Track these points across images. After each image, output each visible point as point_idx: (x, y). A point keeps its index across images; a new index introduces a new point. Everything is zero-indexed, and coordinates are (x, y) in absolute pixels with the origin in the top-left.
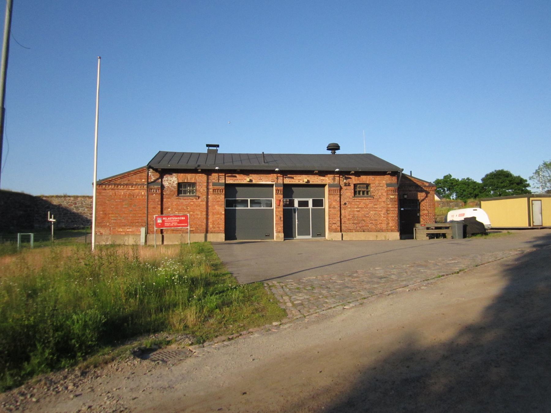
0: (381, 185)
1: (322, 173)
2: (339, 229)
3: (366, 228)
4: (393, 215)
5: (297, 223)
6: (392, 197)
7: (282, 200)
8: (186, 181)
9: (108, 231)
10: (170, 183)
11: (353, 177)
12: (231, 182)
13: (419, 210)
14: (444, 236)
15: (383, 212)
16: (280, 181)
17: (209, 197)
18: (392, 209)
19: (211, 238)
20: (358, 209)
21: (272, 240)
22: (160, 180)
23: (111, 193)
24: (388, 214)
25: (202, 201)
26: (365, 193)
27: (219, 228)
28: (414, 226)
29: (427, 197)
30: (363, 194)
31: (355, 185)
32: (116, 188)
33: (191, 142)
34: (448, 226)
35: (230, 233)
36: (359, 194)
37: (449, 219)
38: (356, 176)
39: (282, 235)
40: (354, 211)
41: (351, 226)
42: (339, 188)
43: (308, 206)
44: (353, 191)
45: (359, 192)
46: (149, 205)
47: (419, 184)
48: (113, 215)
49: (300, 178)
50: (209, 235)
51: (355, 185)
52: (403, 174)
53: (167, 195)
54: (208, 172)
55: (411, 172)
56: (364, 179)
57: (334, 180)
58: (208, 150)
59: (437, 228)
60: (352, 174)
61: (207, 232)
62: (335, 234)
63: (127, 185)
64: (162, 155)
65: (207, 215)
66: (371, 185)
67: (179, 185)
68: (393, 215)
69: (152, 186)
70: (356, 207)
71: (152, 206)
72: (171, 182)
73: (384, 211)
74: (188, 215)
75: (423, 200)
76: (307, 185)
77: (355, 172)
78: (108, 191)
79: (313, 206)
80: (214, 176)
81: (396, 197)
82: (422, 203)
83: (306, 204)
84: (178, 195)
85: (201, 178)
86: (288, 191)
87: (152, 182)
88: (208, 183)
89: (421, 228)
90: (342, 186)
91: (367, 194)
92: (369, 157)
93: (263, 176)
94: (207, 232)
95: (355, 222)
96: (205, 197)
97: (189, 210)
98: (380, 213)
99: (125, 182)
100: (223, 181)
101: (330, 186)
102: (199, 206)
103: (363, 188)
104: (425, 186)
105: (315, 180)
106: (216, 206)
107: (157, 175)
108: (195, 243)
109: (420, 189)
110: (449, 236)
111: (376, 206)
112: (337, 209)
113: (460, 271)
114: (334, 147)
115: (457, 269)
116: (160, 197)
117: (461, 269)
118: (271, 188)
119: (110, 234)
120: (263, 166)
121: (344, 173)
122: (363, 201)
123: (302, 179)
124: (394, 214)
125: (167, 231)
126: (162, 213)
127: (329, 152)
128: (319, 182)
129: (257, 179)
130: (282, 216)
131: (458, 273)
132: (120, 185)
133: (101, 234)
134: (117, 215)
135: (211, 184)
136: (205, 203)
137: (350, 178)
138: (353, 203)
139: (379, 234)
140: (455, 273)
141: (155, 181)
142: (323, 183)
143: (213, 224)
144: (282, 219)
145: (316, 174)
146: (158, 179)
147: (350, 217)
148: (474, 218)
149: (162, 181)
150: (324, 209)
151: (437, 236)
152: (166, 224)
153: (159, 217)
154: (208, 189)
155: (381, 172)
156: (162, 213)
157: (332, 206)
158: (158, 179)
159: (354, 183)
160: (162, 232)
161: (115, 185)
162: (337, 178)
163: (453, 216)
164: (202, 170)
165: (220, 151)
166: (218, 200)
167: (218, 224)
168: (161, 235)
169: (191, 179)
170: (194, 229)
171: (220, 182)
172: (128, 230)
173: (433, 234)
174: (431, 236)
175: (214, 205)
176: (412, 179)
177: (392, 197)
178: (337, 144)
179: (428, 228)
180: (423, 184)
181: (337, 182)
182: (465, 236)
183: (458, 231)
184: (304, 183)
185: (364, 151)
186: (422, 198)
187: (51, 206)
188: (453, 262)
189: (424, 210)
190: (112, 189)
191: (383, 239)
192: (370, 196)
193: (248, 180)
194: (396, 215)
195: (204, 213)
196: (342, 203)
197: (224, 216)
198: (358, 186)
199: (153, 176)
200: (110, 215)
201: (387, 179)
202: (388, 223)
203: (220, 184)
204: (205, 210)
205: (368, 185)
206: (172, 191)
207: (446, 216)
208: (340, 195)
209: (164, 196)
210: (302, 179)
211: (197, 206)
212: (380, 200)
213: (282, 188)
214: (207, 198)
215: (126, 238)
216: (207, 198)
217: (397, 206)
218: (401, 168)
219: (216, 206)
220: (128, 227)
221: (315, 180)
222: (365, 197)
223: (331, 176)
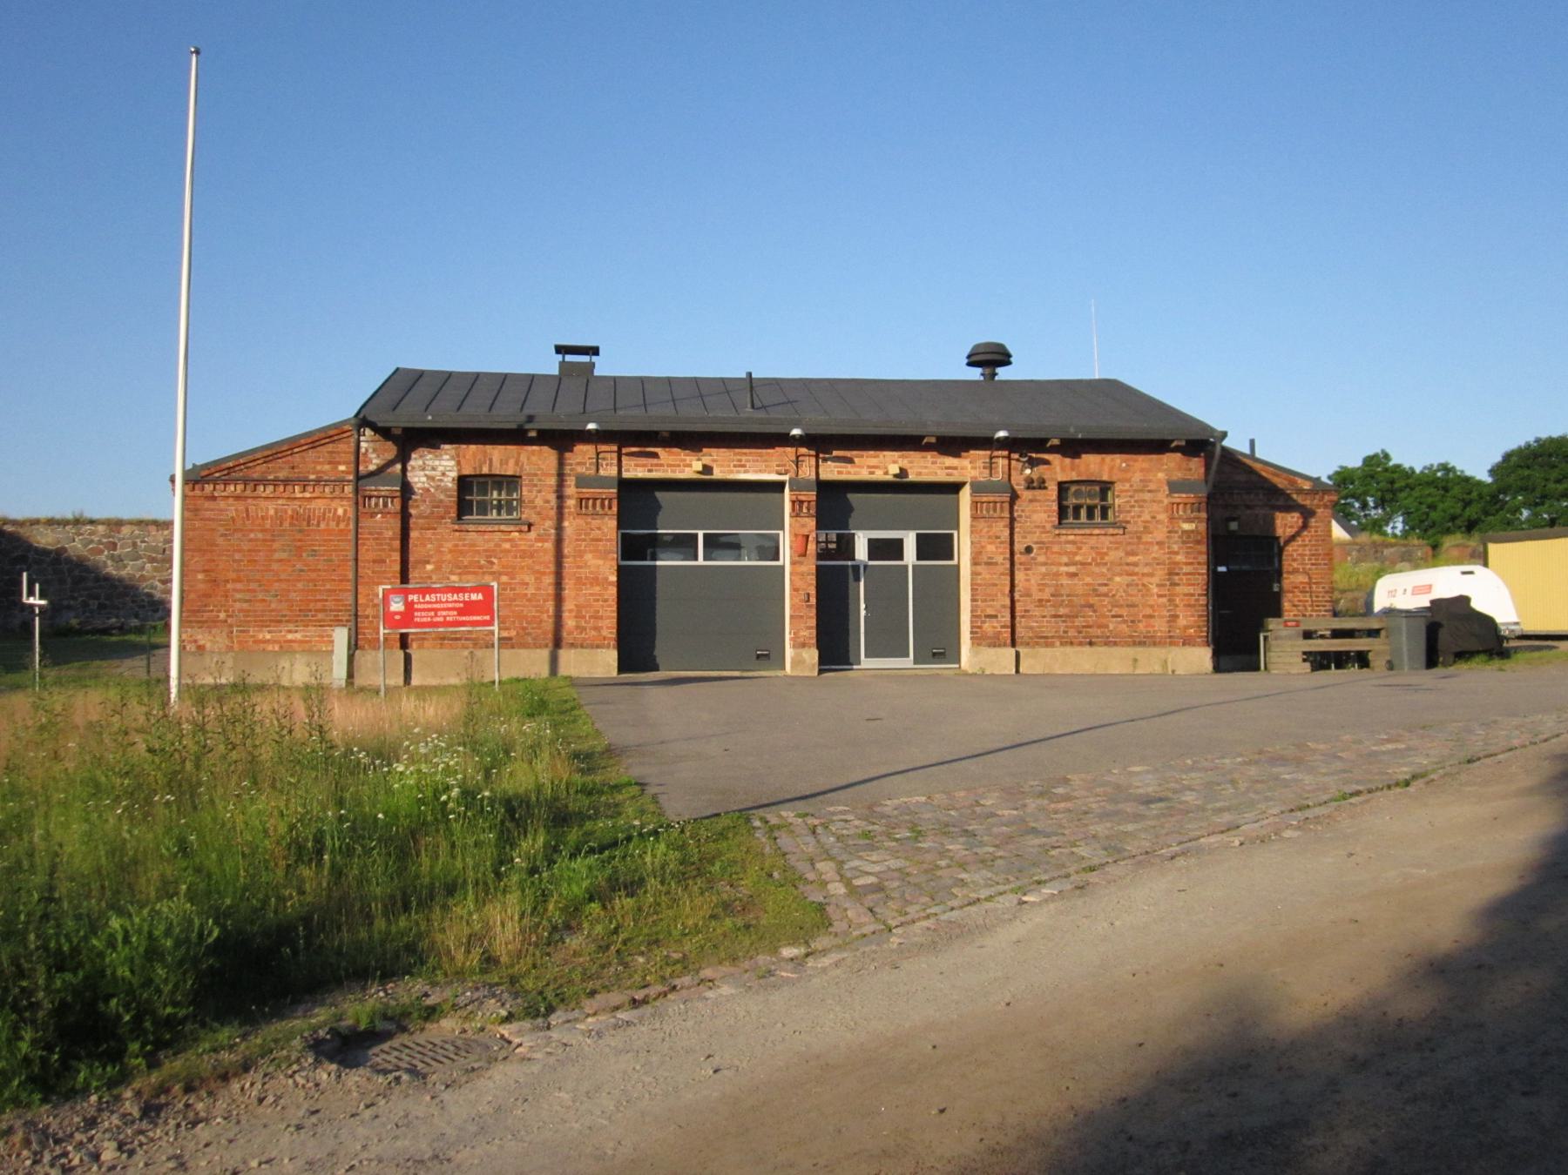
0: (1152, 486)
1: (952, 445)
2: (1006, 634)
3: (1099, 632)
4: (1191, 590)
5: (863, 613)
6: (1186, 526)
7: (813, 535)
8: (485, 470)
9: (222, 640)
11: (1055, 458)
12: (641, 474)
13: (1279, 573)
14: (1362, 660)
15: (1155, 580)
16: (807, 472)
17: (566, 524)
18: (1186, 569)
19: (573, 663)
20: (1072, 569)
21: (780, 673)
22: (399, 466)
23: (232, 509)
24: (1174, 584)
25: (540, 539)
26: (1097, 512)
27: (597, 629)
28: (1260, 626)
29: (1305, 526)
30: (1090, 515)
31: (1063, 488)
32: (248, 493)
33: (502, 338)
34: (1376, 626)
35: (636, 651)
36: (1077, 516)
37: (1379, 604)
38: (1065, 455)
39: (812, 655)
40: (1057, 574)
42: (1006, 497)
43: (901, 557)
44: (1055, 507)
45: (1077, 509)
46: (362, 550)
47: (1280, 482)
48: (239, 586)
49: (873, 461)
50: (565, 655)
51: (1063, 488)
52: (1224, 449)
53: (420, 516)
54: (562, 440)
55: (1252, 443)
56: (1094, 465)
57: (991, 467)
58: (563, 364)
59: (1337, 634)
60: (1053, 450)
61: (557, 643)
62: (992, 651)
63: (286, 482)
64: (404, 383)
65: (559, 584)
66: (1118, 487)
67: (464, 483)
68: (1191, 590)
69: (370, 488)
70: (1064, 561)
71: (371, 556)
72: (437, 474)
73: (1161, 573)
74: (495, 585)
75: (1293, 538)
76: (901, 485)
77: (1062, 440)
78: (222, 504)
79: (919, 558)
80: (583, 455)
81: (1203, 527)
82: (1289, 548)
83: (891, 549)
84: (459, 517)
85: (536, 462)
86: (833, 503)
87: (372, 474)
88: (561, 476)
89: (1285, 632)
90: (1020, 487)
91: (1104, 515)
92: (1111, 390)
93: (748, 455)
94: (557, 643)
95: (1062, 611)
96: (549, 524)
97: (495, 568)
98: (1146, 580)
99: (282, 475)
100: (613, 471)
101: (978, 488)
102: (532, 556)
103: (1090, 496)
104: (1300, 491)
105: (926, 467)
106: (588, 557)
107: (390, 450)
108: (518, 680)
109: (1281, 502)
110: (1378, 662)
112: (1001, 569)
113: (1415, 777)
114: (991, 358)
115: (1404, 772)
116: (396, 523)
117: (1418, 771)
118: (777, 495)
119: (230, 649)
120: (747, 418)
121: (1026, 446)
122: (1088, 542)
123: (883, 466)
125: (422, 638)
126: (404, 578)
127: (976, 374)
128: (941, 477)
129: (727, 465)
130: (813, 592)
131: (1407, 784)
132: (264, 482)
133: (201, 648)
134: (253, 586)
135: (571, 482)
136: (549, 545)
137: (1047, 462)
138: (1056, 548)
140: (1397, 784)
141: (381, 470)
142: (955, 477)
143: (578, 616)
144: (813, 601)
145: (928, 448)
146: (391, 463)
147: (1046, 595)
148: (1463, 601)
149: (404, 470)
150: (958, 567)
151: (1340, 660)
152: (419, 617)
153: (395, 591)
154: (561, 498)
155: (1152, 441)
156: (404, 578)
158: (391, 463)
159: (1061, 478)
160: (404, 642)
161: (246, 482)
162: (1001, 463)
163: (1392, 593)
164: (541, 433)
165: (604, 367)
167: (596, 617)
168: (401, 654)
169: (504, 462)
170: (513, 633)
171: (602, 472)
172: (290, 636)
173: (1324, 654)
174: (1320, 661)
175: (580, 554)
176: (1257, 466)
177: (1186, 526)
178: (1002, 346)
179: (1308, 635)
180: (1293, 483)
181: (999, 476)
182: (1431, 663)
183: (1410, 644)
184: (889, 478)
185: (1095, 370)
186: (1290, 532)
187: (31, 555)
188: (1390, 746)
189: (1295, 571)
190: (238, 498)
191: (1158, 669)
192: (1114, 525)
193: (698, 466)
195: (549, 580)
196: (1019, 547)
197: (613, 591)
198: (1073, 488)
199: (374, 452)
200: (229, 586)
201: (1170, 466)
203: (602, 482)
204: (552, 568)
205: (1105, 487)
206: (438, 504)
207: (1371, 594)
208: (1012, 520)
209: (412, 521)
210: (883, 466)
211: (524, 554)
214: (559, 529)
215: (284, 663)
217: (1203, 558)
218: (1220, 428)
219: (588, 557)
220: (291, 626)
221: (926, 467)
222: (1097, 526)
223: (981, 455)
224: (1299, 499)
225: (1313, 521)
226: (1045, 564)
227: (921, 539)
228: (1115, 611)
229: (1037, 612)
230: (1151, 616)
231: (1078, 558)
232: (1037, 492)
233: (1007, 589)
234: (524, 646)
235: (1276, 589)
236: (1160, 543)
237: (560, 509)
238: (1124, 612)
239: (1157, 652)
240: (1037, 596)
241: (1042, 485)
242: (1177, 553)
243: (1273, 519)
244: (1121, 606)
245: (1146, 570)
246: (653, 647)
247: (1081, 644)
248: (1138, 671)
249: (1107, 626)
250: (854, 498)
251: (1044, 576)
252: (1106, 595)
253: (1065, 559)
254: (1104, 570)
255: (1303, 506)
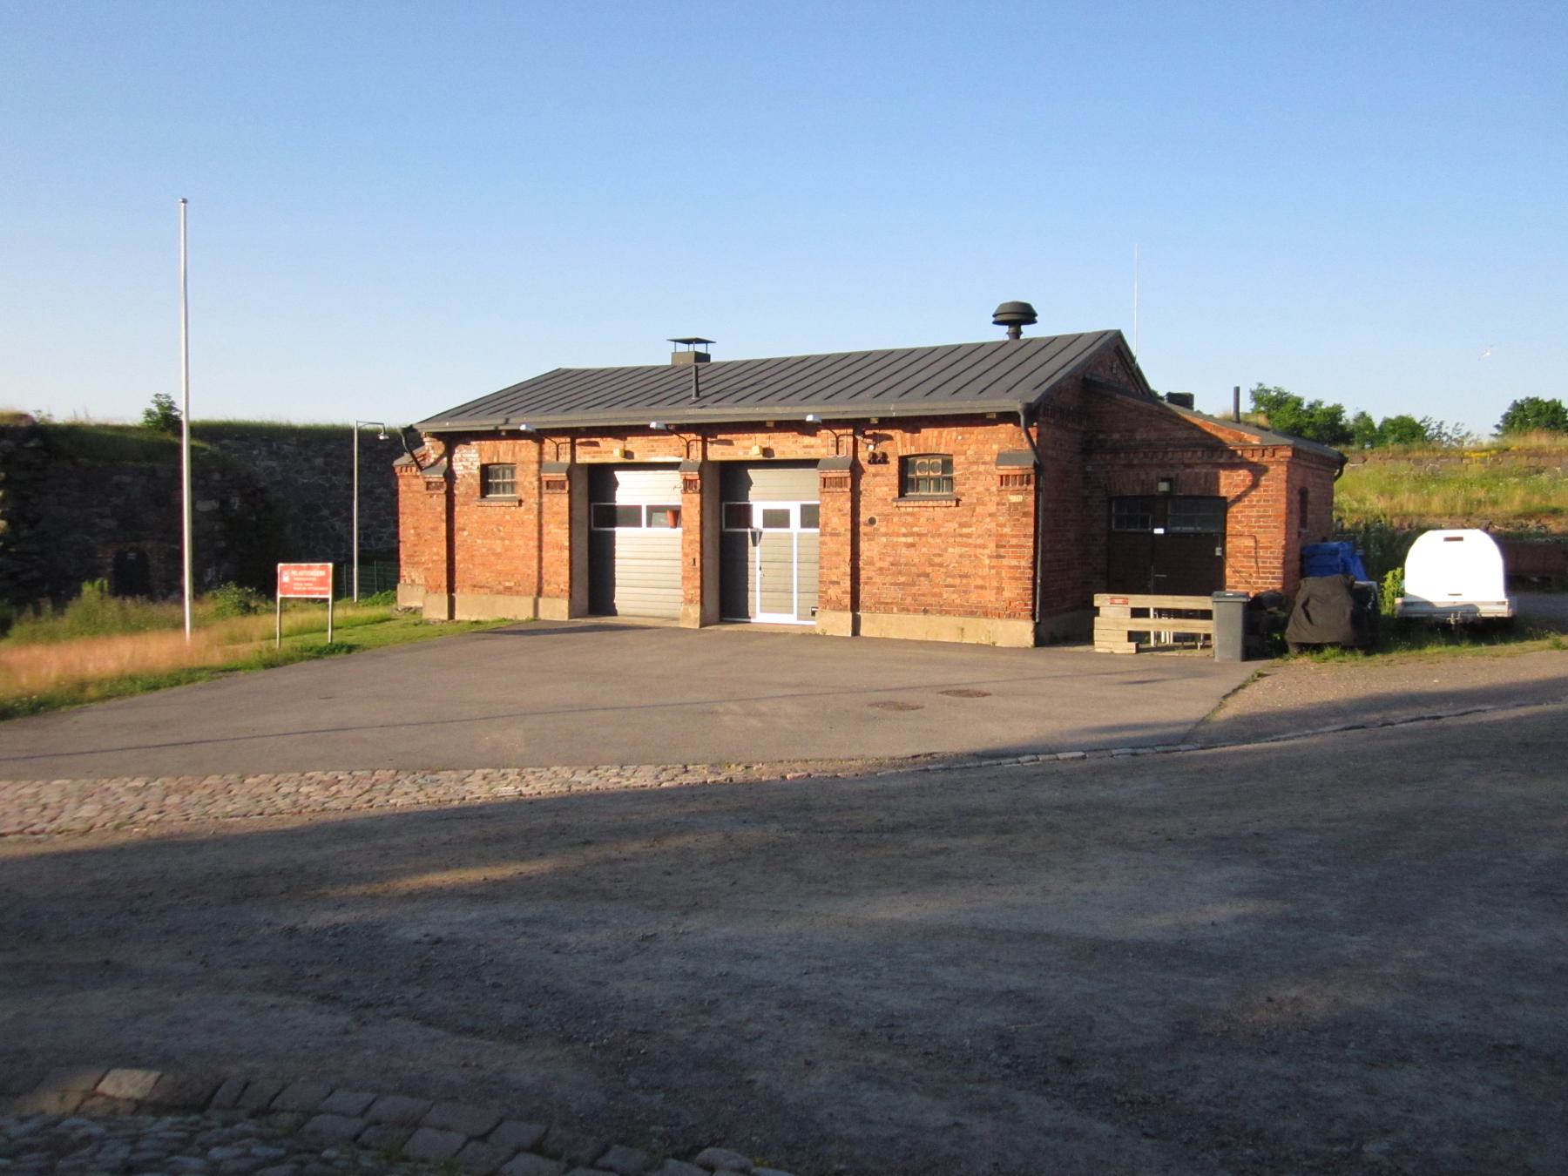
0: (987, 458)
2: (847, 600)
4: (1014, 562)
5: (758, 573)
6: (1015, 499)
10: (465, 467)
11: (897, 434)
13: (1224, 536)
15: (987, 551)
20: (910, 540)
24: (999, 557)
29: (1255, 485)
31: (904, 461)
38: (905, 431)
40: (894, 546)
41: (890, 594)
42: (847, 473)
44: (896, 481)
49: (747, 443)
54: (539, 436)
56: (932, 439)
58: (675, 355)
61: (540, 593)
65: (540, 548)
66: (955, 460)
67: (485, 470)
70: (899, 529)
75: (1239, 499)
79: (803, 525)
80: (549, 445)
82: (1233, 510)
84: (483, 496)
85: (528, 449)
87: (432, 465)
90: (864, 463)
95: (902, 579)
96: (532, 502)
98: (979, 551)
100: (568, 458)
103: (932, 468)
111: (965, 530)
114: (1019, 315)
116: (443, 500)
122: (926, 511)
124: (1021, 558)
127: (1002, 333)
130: (698, 557)
137: (890, 438)
138: (896, 519)
139: (969, 623)
141: (437, 462)
142: (812, 455)
146: (441, 457)
147: (885, 565)
149: (450, 462)
157: (829, 529)
164: (508, 432)
166: (556, 508)
167: (558, 574)
169: (506, 454)
171: (561, 460)
176: (1197, 421)
177: (1015, 499)
194: (1026, 562)
196: (863, 518)
202: (1000, 590)
205: (947, 464)
206: (470, 486)
212: (979, 509)
213: (695, 475)
214: (540, 505)
216: (540, 505)
224: (1248, 455)
225: (1263, 480)
226: (886, 535)
227: (804, 509)
228: (949, 581)
229: (878, 579)
230: (982, 587)
231: (916, 529)
232: (880, 467)
233: (848, 558)
234: (518, 593)
235: (1218, 553)
236: (990, 515)
237: (540, 487)
238: (957, 581)
239: (984, 622)
240: (879, 564)
241: (884, 460)
242: (1004, 526)
243: (1217, 478)
244: (953, 577)
245: (979, 541)
246: (613, 596)
247: (915, 611)
248: (966, 641)
249: (941, 595)
250: (751, 472)
251: (885, 546)
252: (941, 565)
253: (904, 530)
254: (938, 540)
255: (1255, 464)
